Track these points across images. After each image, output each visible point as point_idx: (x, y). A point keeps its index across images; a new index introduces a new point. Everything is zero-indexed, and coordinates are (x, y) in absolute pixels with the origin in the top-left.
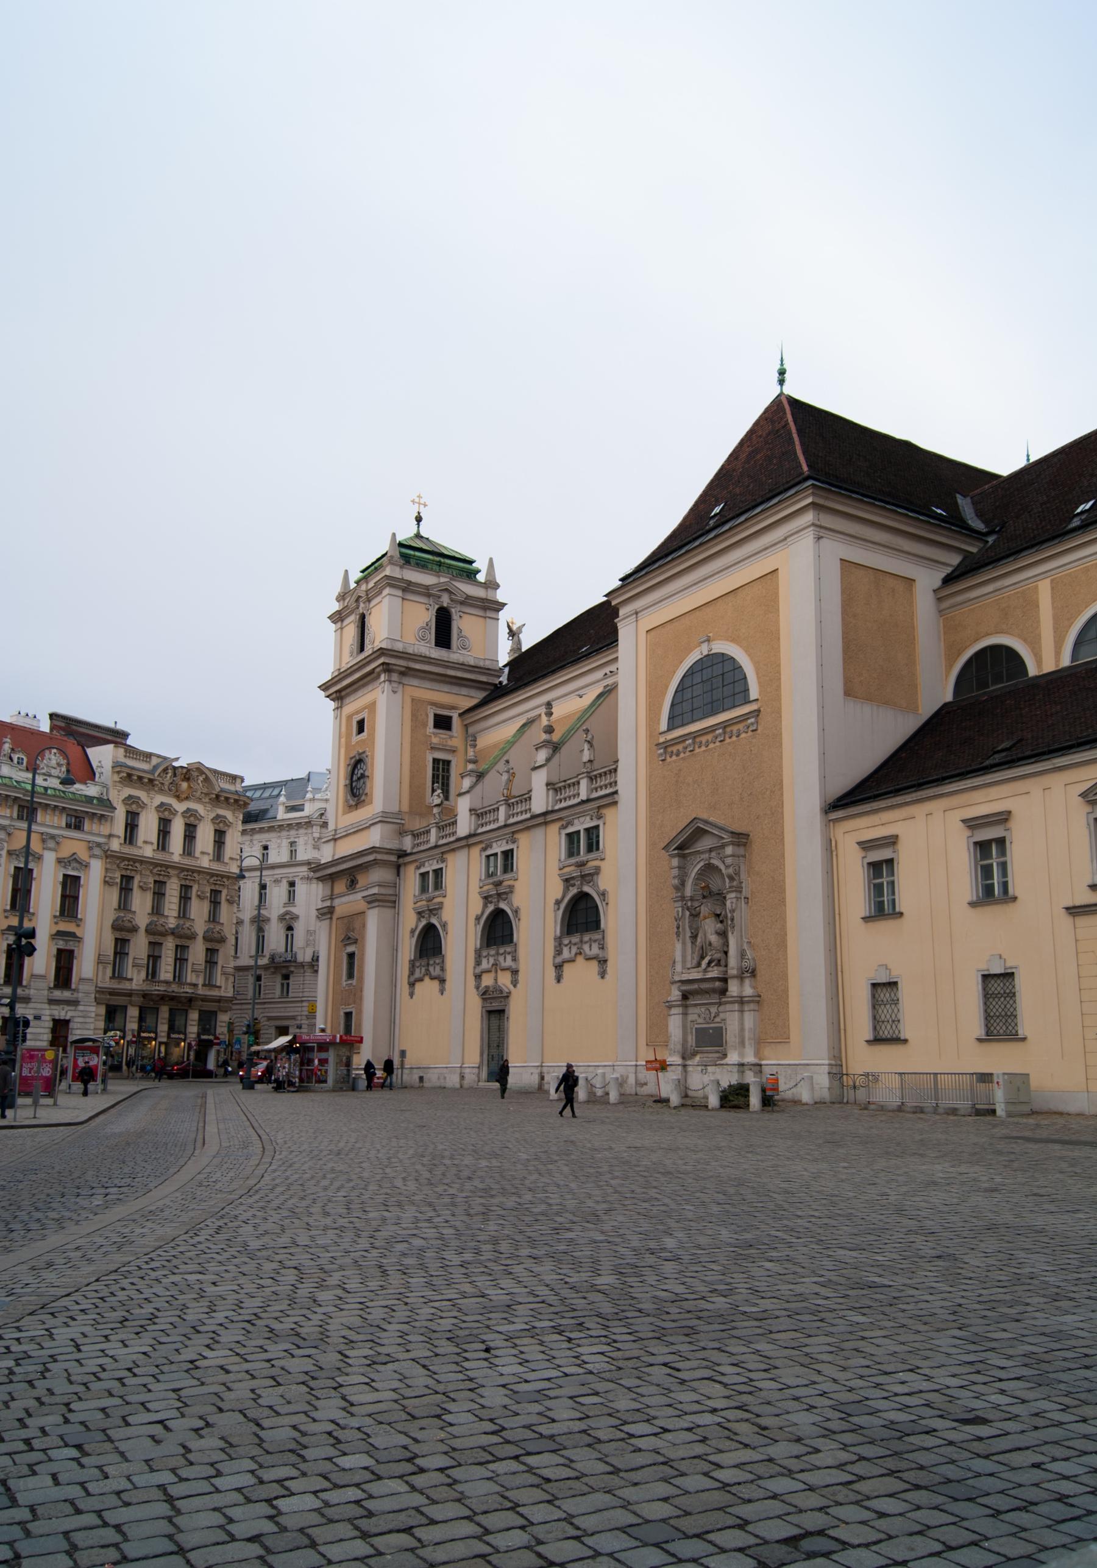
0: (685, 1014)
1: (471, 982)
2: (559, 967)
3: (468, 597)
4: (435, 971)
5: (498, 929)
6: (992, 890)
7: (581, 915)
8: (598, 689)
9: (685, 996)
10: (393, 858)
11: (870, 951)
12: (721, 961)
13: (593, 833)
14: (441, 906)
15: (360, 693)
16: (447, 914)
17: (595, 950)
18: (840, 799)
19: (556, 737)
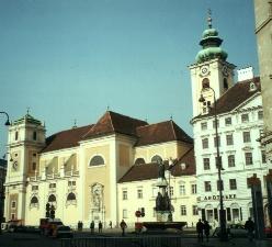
6: (140, 196)
7: (71, 197)
13: (74, 183)
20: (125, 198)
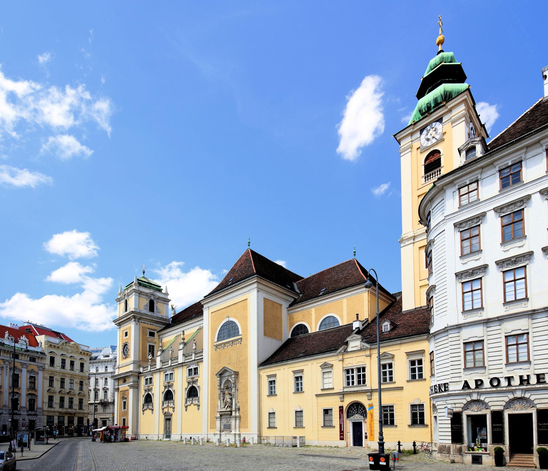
0: (221, 420)
1: (161, 410)
2: (186, 407)
3: (159, 297)
4: (150, 407)
5: (169, 396)
7: (192, 392)
8: (198, 328)
9: (221, 416)
10: (137, 374)
11: (269, 404)
12: (231, 407)
13: (196, 369)
14: (152, 389)
15: (126, 324)
16: (154, 391)
17: (196, 402)
18: (262, 363)
19: (185, 341)
20: (272, 393)
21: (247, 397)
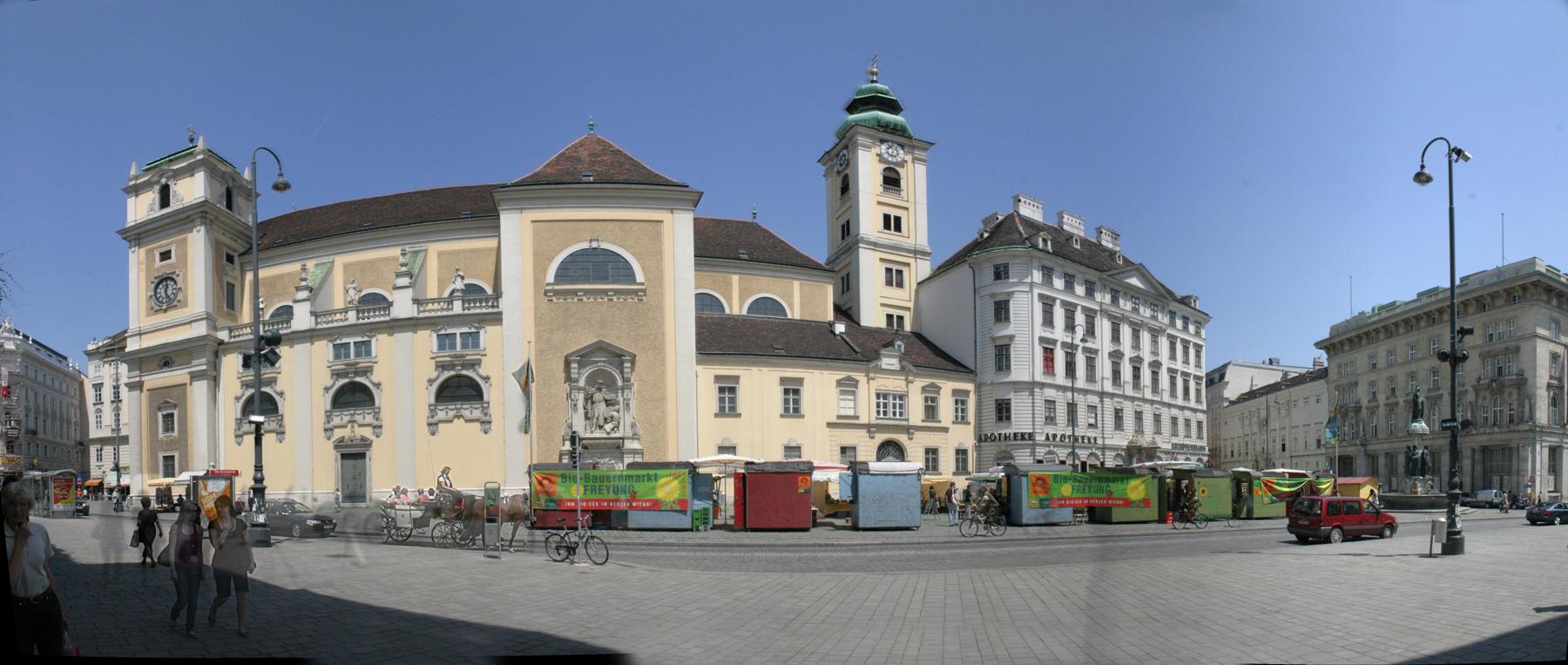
2: (433, 426)
5: (352, 394)
7: (459, 390)
17: (477, 414)
21: (663, 412)
